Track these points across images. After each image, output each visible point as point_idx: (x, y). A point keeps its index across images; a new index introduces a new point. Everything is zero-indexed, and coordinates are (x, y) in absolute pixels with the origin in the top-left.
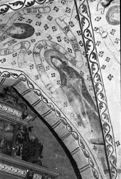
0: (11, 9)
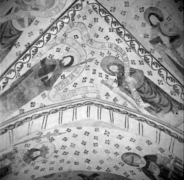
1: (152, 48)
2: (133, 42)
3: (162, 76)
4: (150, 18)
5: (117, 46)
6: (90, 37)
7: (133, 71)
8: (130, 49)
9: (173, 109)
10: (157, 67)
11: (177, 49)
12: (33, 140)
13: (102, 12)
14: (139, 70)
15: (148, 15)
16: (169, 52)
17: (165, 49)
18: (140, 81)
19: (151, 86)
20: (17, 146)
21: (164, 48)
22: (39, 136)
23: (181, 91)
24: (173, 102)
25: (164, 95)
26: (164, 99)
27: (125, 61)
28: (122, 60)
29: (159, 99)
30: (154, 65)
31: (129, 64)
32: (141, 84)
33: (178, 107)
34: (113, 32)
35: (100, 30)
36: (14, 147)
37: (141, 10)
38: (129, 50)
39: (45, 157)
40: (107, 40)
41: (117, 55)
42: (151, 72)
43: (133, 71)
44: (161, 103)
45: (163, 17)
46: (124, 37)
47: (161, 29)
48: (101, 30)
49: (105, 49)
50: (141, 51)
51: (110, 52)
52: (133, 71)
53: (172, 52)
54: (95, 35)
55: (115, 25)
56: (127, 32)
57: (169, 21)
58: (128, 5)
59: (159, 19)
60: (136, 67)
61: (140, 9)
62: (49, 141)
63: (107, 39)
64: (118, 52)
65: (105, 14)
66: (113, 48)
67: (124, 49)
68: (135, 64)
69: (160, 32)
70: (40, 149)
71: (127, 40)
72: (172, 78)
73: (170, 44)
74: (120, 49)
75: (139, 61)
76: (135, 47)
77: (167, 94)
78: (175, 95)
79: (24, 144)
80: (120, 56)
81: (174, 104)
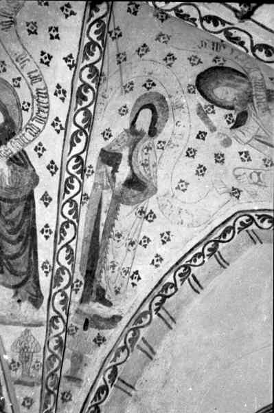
0: (252, 42)
1: (94, 165)
2: (81, 135)
3: (62, 234)
4: (143, 111)
5: (47, 93)
6: (16, 12)
7: (23, 162)
8: (62, 128)
9: (19, 290)
10: (70, 213)
11: (121, 205)
13: (96, 29)
14: (34, 170)
15: (147, 103)
16: (107, 197)
17: (107, 188)
18: (15, 189)
19: (26, 220)
21: (109, 184)
23: (65, 285)
24: (31, 279)
25: (30, 256)
26: (25, 262)
27: (29, 130)
28: (25, 123)
29: (15, 252)
30: (71, 206)
31: (30, 141)
32: (13, 197)
33: (33, 295)
34: (71, 69)
35: (52, 32)
37: (148, 83)
38: (58, 128)
40: (41, 60)
41: (29, 104)
42: (50, 199)
43: (23, 162)
44: (11, 262)
45: (160, 132)
46: (79, 111)
47: (137, 146)
48: (55, 34)
49: (17, 68)
50: (76, 161)
51: (22, 83)
52: (23, 158)
53: (111, 203)
54: (31, 25)
55: (89, 76)
56: (91, 109)
57: (158, 148)
58: (143, 54)
59: (150, 128)
60: (39, 165)
61: (149, 81)
63: (45, 61)
64: (36, 102)
65: (98, 38)
66: (34, 88)
67: (50, 113)
68: (40, 155)
69: (130, 151)
71: (77, 121)
72: (73, 254)
73: (121, 187)
74: (45, 105)
75: (52, 162)
76: (75, 145)
77: (37, 258)
78: (47, 272)
80: (30, 110)
81: (30, 284)
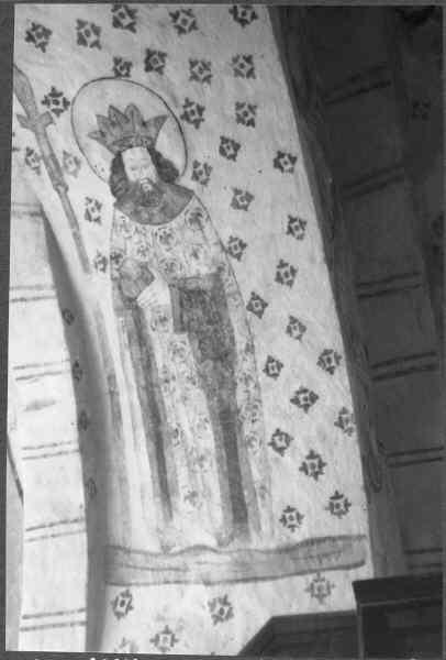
12: (67, 189)
20: (92, 256)
22: (47, 164)
36: (94, 270)
39: (160, 121)
62: (65, 116)
70: (111, 151)
79: (86, 227)
